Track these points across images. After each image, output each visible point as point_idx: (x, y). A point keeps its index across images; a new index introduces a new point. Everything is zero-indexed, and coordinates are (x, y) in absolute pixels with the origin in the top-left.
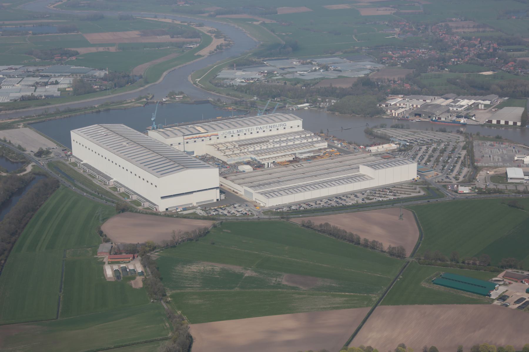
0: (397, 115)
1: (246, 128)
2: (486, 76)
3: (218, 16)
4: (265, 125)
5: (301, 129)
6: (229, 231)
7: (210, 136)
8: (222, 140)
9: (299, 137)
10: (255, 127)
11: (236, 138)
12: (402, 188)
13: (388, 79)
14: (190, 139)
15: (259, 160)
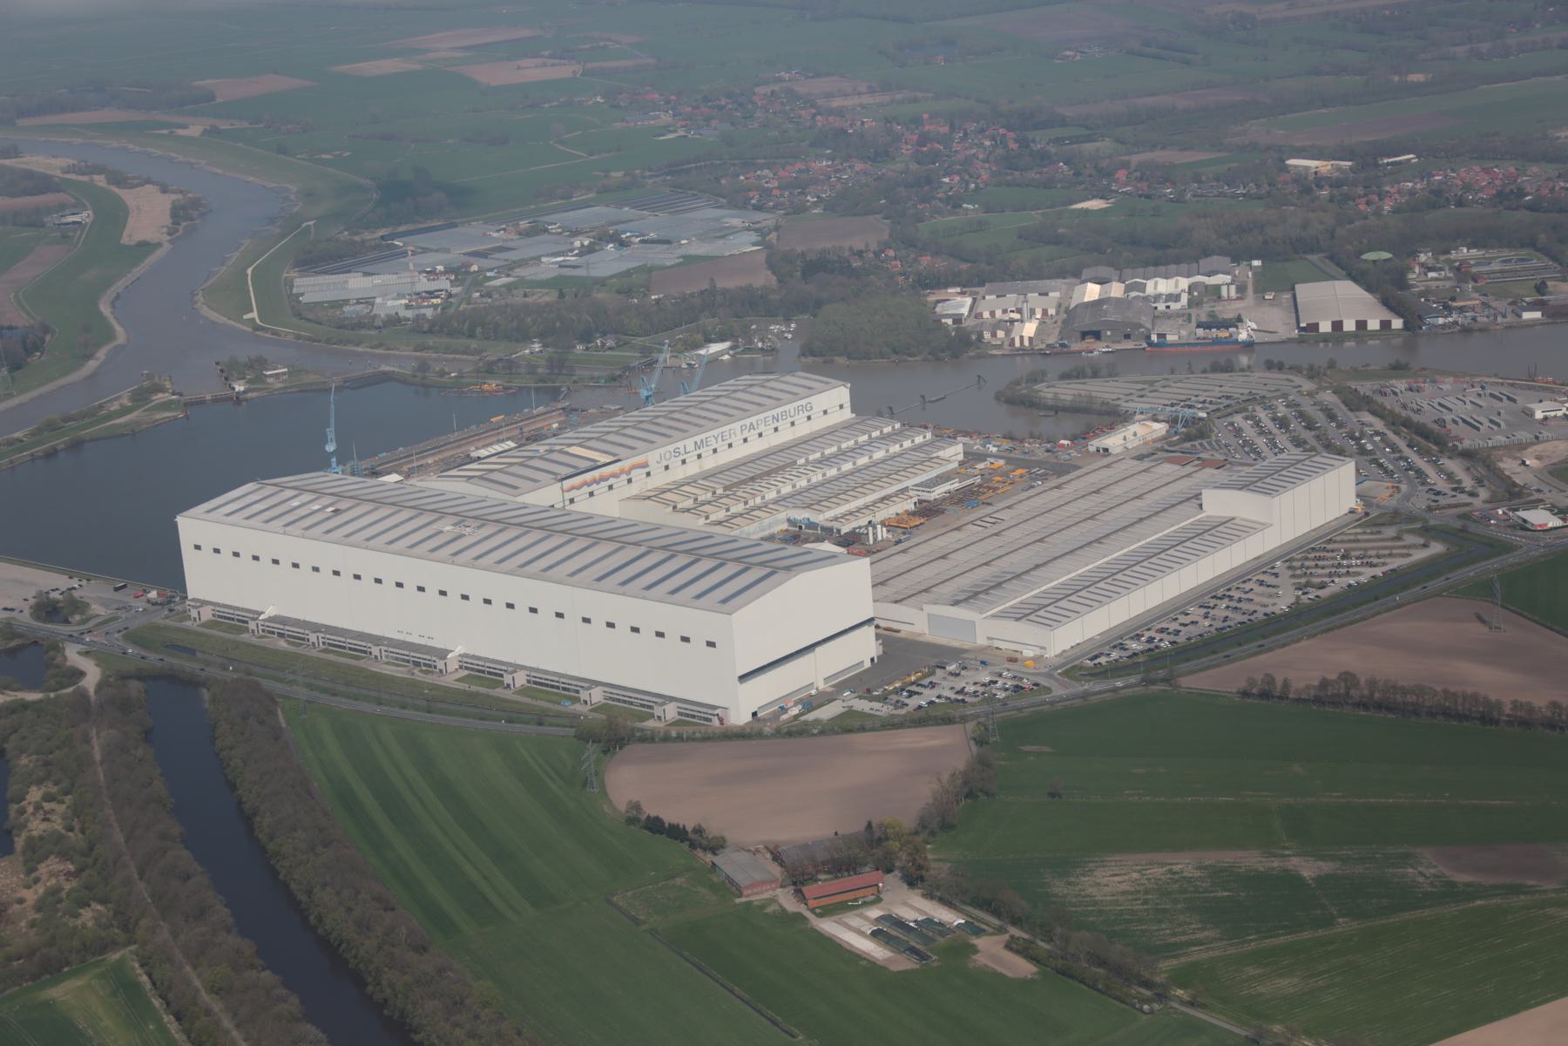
0: (1026, 343)
1: (715, 432)
3: (21, 122)
4: (762, 416)
5: (847, 414)
6: (1047, 749)
7: (629, 472)
8: (660, 480)
9: (865, 437)
10: (737, 426)
11: (693, 468)
12: (1358, 541)
13: (851, 249)
14: (578, 488)
15: (829, 524)
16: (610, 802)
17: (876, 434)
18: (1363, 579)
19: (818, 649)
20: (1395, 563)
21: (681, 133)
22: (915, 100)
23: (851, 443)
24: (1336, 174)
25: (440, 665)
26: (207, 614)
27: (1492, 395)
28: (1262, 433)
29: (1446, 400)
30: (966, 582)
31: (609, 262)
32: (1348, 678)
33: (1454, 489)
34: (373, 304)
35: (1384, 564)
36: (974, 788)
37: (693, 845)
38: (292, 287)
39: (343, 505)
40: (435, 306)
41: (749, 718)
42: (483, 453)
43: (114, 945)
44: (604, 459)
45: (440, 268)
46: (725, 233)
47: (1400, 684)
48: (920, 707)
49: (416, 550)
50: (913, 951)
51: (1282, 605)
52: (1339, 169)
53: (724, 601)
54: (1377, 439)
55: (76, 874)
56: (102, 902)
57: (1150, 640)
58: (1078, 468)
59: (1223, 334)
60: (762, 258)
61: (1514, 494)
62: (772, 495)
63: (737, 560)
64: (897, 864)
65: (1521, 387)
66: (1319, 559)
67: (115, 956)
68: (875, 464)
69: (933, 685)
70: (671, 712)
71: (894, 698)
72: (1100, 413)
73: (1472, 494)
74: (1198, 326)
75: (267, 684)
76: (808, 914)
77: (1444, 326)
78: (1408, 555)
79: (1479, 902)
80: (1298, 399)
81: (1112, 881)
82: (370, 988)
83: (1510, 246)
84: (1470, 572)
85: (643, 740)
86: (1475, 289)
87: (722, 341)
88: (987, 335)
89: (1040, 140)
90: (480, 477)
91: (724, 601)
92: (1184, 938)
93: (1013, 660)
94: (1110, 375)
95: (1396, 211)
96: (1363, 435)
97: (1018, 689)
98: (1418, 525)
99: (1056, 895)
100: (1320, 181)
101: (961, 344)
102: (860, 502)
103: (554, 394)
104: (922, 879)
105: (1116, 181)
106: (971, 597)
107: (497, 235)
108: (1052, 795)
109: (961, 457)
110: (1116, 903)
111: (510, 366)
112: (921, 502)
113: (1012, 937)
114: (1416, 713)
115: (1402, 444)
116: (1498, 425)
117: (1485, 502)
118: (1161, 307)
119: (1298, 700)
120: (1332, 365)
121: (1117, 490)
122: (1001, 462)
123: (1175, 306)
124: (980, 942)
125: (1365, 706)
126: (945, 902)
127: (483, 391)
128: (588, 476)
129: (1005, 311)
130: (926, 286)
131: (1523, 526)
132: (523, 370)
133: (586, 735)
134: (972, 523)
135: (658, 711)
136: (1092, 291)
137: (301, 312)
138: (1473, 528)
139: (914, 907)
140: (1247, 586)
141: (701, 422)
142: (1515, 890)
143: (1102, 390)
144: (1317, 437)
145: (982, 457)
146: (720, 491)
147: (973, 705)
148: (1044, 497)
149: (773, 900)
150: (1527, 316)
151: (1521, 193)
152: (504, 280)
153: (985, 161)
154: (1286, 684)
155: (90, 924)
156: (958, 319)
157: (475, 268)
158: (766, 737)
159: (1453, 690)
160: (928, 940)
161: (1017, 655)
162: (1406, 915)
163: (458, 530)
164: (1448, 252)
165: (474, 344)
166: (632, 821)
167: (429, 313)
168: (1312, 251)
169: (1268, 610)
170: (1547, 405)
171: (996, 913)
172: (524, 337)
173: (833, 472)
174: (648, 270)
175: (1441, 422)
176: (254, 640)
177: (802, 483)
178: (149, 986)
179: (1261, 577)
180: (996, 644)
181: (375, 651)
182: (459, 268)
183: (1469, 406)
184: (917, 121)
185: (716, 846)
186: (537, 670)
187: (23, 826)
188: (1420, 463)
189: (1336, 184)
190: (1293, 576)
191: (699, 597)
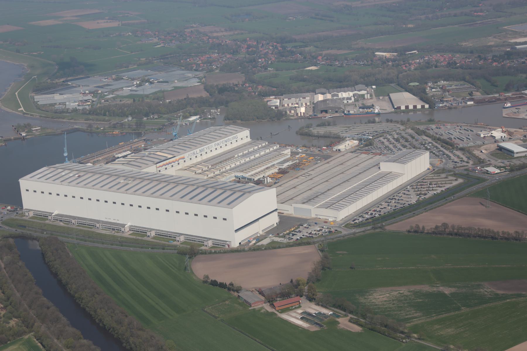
0: (302, 115)
2: (311, 70)
5: (249, 139)
6: (345, 252)
7: (178, 161)
8: (189, 163)
9: (257, 147)
10: (213, 144)
11: (199, 159)
12: (433, 179)
13: (233, 84)
14: (162, 166)
15: (250, 177)
16: (195, 276)
17: (260, 146)
18: (439, 192)
19: (260, 220)
20: (448, 186)
21: (162, 45)
22: (242, 34)
23: (252, 149)
24: (393, 57)
25: (123, 229)
26: (31, 214)
27: (465, 129)
28: (391, 143)
29: (450, 131)
30: (305, 195)
31: (148, 89)
32: (445, 225)
33: (461, 161)
34: (65, 105)
35: (444, 186)
36: (324, 267)
37: (229, 289)
38: (34, 99)
39: (81, 174)
40: (89, 105)
41: (238, 245)
42: (120, 155)
43: (25, 333)
45: (87, 92)
46: (187, 79)
47: (463, 227)
48: (297, 239)
49: (112, 189)
50: (317, 324)
51: (414, 200)
52: (393, 55)
53: (229, 204)
54: (430, 144)
55: (5, 307)
56: (16, 317)
57: (371, 214)
58: (332, 157)
59: (369, 111)
60: (202, 87)
61: (480, 162)
62: (228, 168)
63: (230, 190)
64: (304, 293)
65: (474, 127)
66: (422, 185)
67: (26, 337)
68: (262, 156)
69: (300, 232)
70: (210, 243)
71: (288, 236)
72: (334, 138)
73: (467, 162)
74: (360, 108)
75: (60, 238)
76: (276, 312)
77: (442, 107)
78: (451, 183)
79: (508, 300)
80: (400, 132)
81: (380, 297)
82: (124, 344)
83: (457, 80)
84: (474, 188)
85: (202, 253)
86: (449, 95)
87: (195, 115)
88: (288, 112)
89: (289, 47)
90: (127, 163)
91: (229, 204)
92: (410, 316)
93: (326, 222)
94: (334, 125)
95: (415, 69)
96: (425, 143)
97: (330, 232)
98: (452, 173)
99: (362, 303)
100: (388, 60)
101: (279, 115)
102: (259, 170)
103: (139, 135)
104: (315, 299)
105: (319, 60)
107: (105, 81)
108: (351, 268)
109: (290, 153)
110: (384, 305)
111: (122, 125)
112: (280, 169)
113: (351, 318)
114: (469, 236)
115: (439, 146)
116: (470, 139)
117: (472, 165)
118: (345, 102)
119: (428, 233)
121: (349, 163)
122: (304, 155)
123: (350, 102)
124: (340, 320)
125: (451, 235)
126: (326, 307)
127: (113, 134)
128: (165, 162)
129: (292, 104)
130: (263, 96)
131: (487, 172)
132: (127, 127)
133: (182, 253)
134: (301, 175)
135: (205, 243)
136: (320, 97)
137: (39, 108)
138: (471, 174)
139: (314, 309)
140: (400, 195)
141: (201, 143)
142: (520, 296)
144: (410, 144)
145: (298, 153)
146: (210, 167)
147: (316, 238)
149: (263, 308)
150: (469, 103)
151: (456, 63)
152: (111, 96)
153: (272, 54)
154: (423, 228)
155: (15, 325)
156: (276, 107)
157: (100, 92)
158: (246, 251)
159: (481, 228)
160: (321, 320)
161: (327, 220)
162: (484, 306)
163: (126, 182)
164: (436, 83)
165: (107, 118)
166: (205, 282)
167: (87, 107)
168: (391, 83)
169: (410, 203)
170: (484, 132)
171: (345, 311)
172: (124, 115)
173: (248, 159)
174: (163, 92)
175: (451, 139)
176: (51, 223)
177: (238, 163)
178: (41, 347)
179: (404, 192)
180: (319, 217)
181: (98, 225)
182: (94, 92)
183: (458, 133)
184: (245, 41)
185: (238, 290)
186: (159, 230)
188: (447, 152)
189: (394, 60)
190: (414, 191)
191: (219, 203)
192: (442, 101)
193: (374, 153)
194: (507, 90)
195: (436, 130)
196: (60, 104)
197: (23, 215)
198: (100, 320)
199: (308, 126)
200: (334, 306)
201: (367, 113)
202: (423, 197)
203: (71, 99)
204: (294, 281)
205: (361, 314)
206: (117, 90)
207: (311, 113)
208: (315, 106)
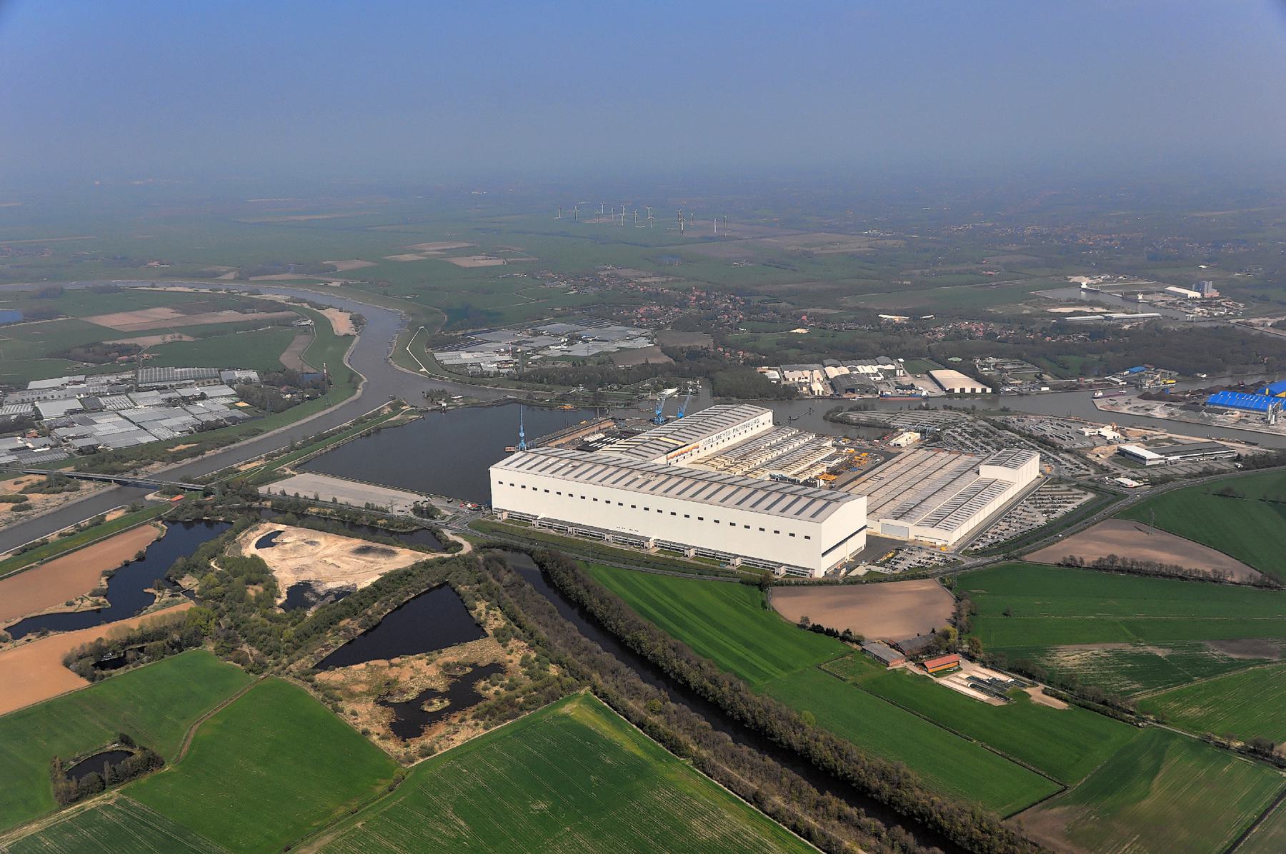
5: (771, 425)
8: (703, 454)
11: (715, 449)
20: (1079, 502)
25: (646, 544)
31: (580, 350)
32: (1113, 558)
37: (844, 639)
39: (577, 464)
42: (591, 439)
43: (581, 686)
44: (681, 444)
51: (1042, 520)
55: (531, 647)
60: (658, 350)
61: (1103, 470)
67: (583, 692)
81: (1069, 658)
84: (1116, 506)
100: (900, 326)
103: (602, 412)
106: (902, 514)
107: (522, 336)
120: (974, 408)
121: (928, 464)
124: (1028, 690)
125: (1122, 571)
133: (747, 583)
136: (833, 372)
139: (985, 674)
143: (880, 416)
145: (843, 448)
148: (892, 469)
149: (905, 669)
156: (779, 381)
166: (802, 627)
171: (1030, 676)
174: (607, 353)
184: (689, 290)
187: (485, 622)
189: (909, 326)
192: (1007, 385)
193: (950, 452)
194: (1084, 373)
195: (1021, 424)
196: (472, 365)
197: (493, 514)
198: (679, 675)
199: (838, 410)
200: (1010, 670)
201: (910, 395)
202: (1052, 516)
203: (487, 357)
204: (937, 631)
205: (1060, 683)
206: (542, 348)
207: (830, 392)
208: (832, 383)
